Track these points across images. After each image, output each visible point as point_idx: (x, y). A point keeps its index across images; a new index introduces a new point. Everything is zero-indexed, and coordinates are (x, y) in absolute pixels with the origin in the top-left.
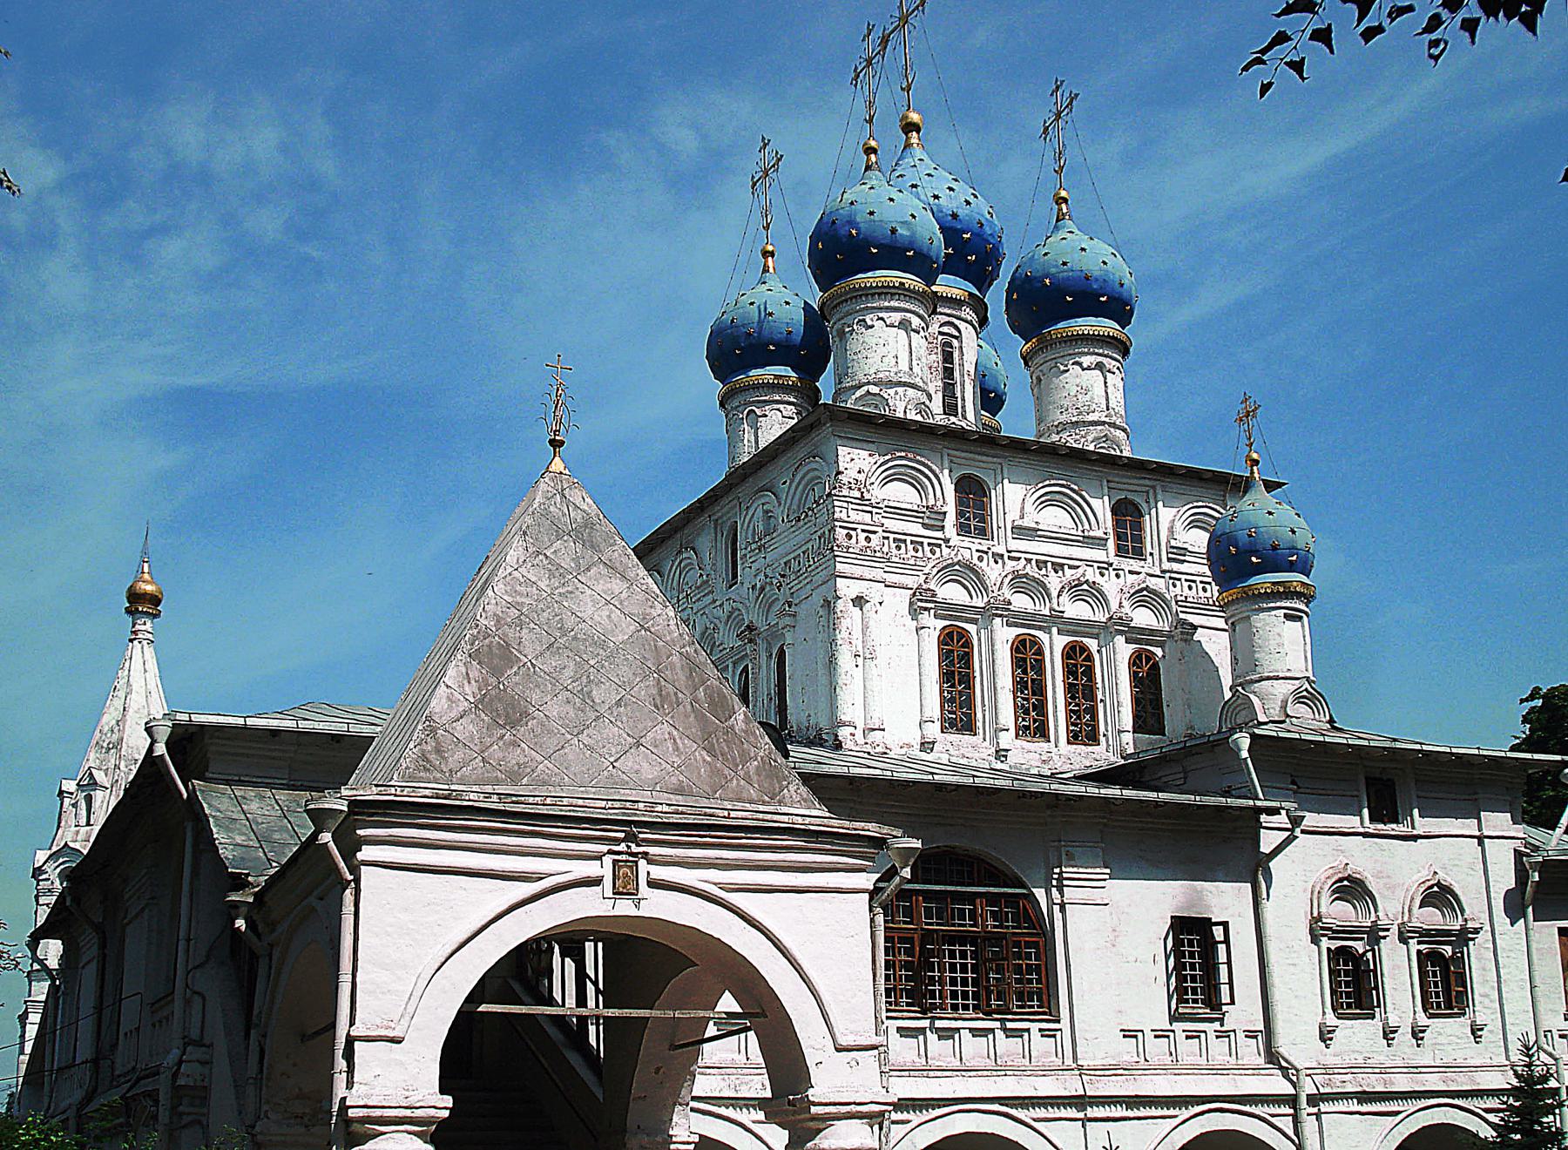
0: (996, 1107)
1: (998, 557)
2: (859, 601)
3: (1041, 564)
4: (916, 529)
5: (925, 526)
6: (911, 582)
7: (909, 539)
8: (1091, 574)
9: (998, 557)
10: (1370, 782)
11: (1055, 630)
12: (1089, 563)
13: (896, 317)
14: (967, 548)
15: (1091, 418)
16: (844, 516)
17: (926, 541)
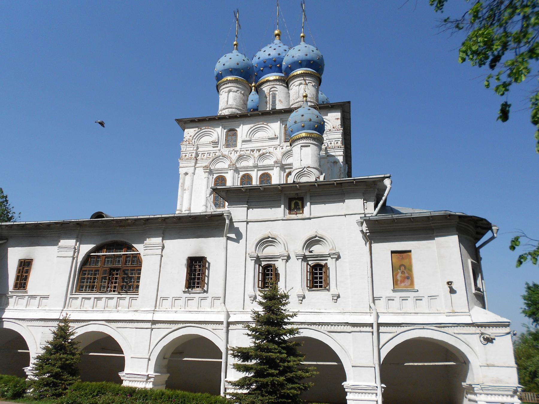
0: (103, 323)
1: (236, 151)
2: (186, 174)
3: (253, 151)
4: (210, 148)
5: (213, 147)
6: (204, 165)
7: (206, 152)
8: (271, 150)
9: (236, 151)
10: (290, 200)
11: (256, 170)
12: (270, 147)
13: (227, 89)
14: (226, 151)
15: (297, 100)
16: (184, 150)
17: (212, 152)
